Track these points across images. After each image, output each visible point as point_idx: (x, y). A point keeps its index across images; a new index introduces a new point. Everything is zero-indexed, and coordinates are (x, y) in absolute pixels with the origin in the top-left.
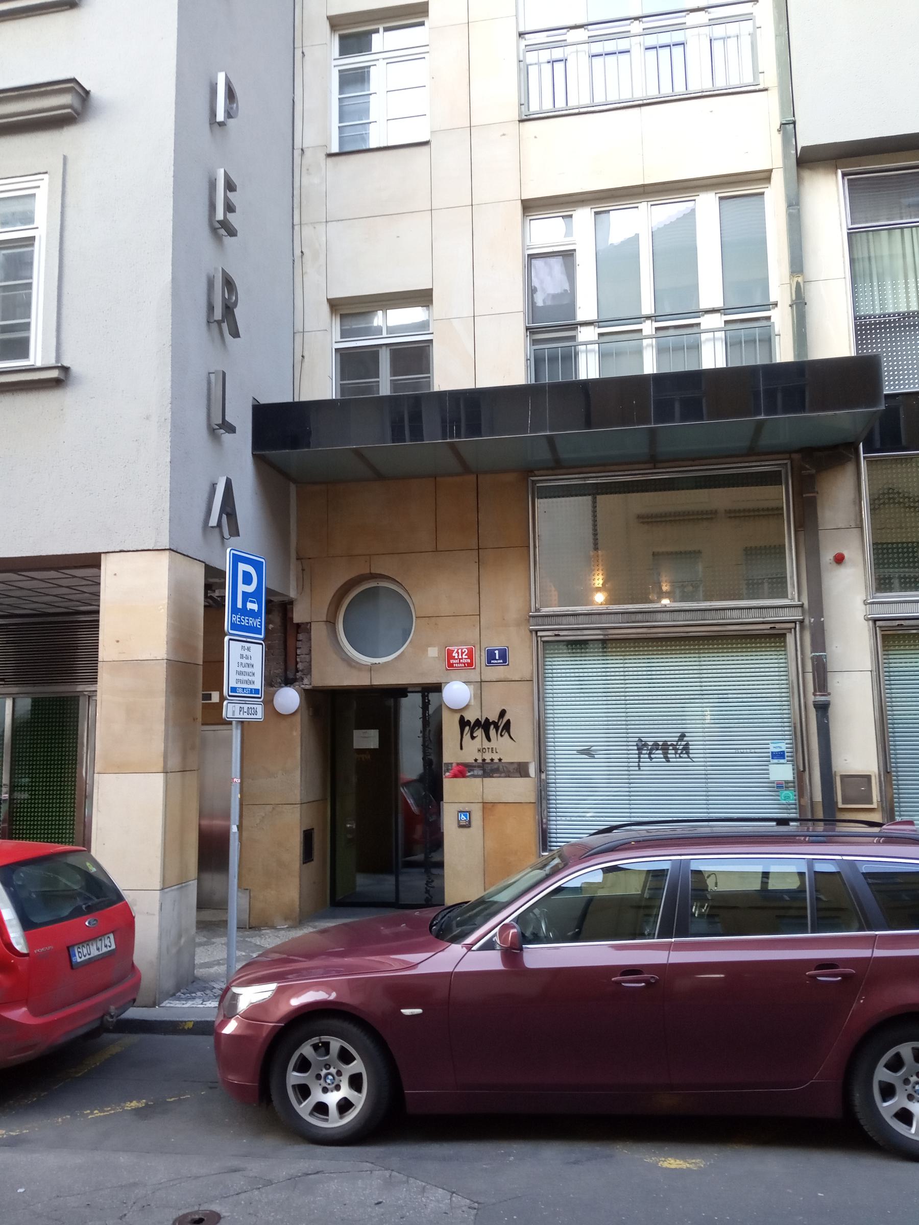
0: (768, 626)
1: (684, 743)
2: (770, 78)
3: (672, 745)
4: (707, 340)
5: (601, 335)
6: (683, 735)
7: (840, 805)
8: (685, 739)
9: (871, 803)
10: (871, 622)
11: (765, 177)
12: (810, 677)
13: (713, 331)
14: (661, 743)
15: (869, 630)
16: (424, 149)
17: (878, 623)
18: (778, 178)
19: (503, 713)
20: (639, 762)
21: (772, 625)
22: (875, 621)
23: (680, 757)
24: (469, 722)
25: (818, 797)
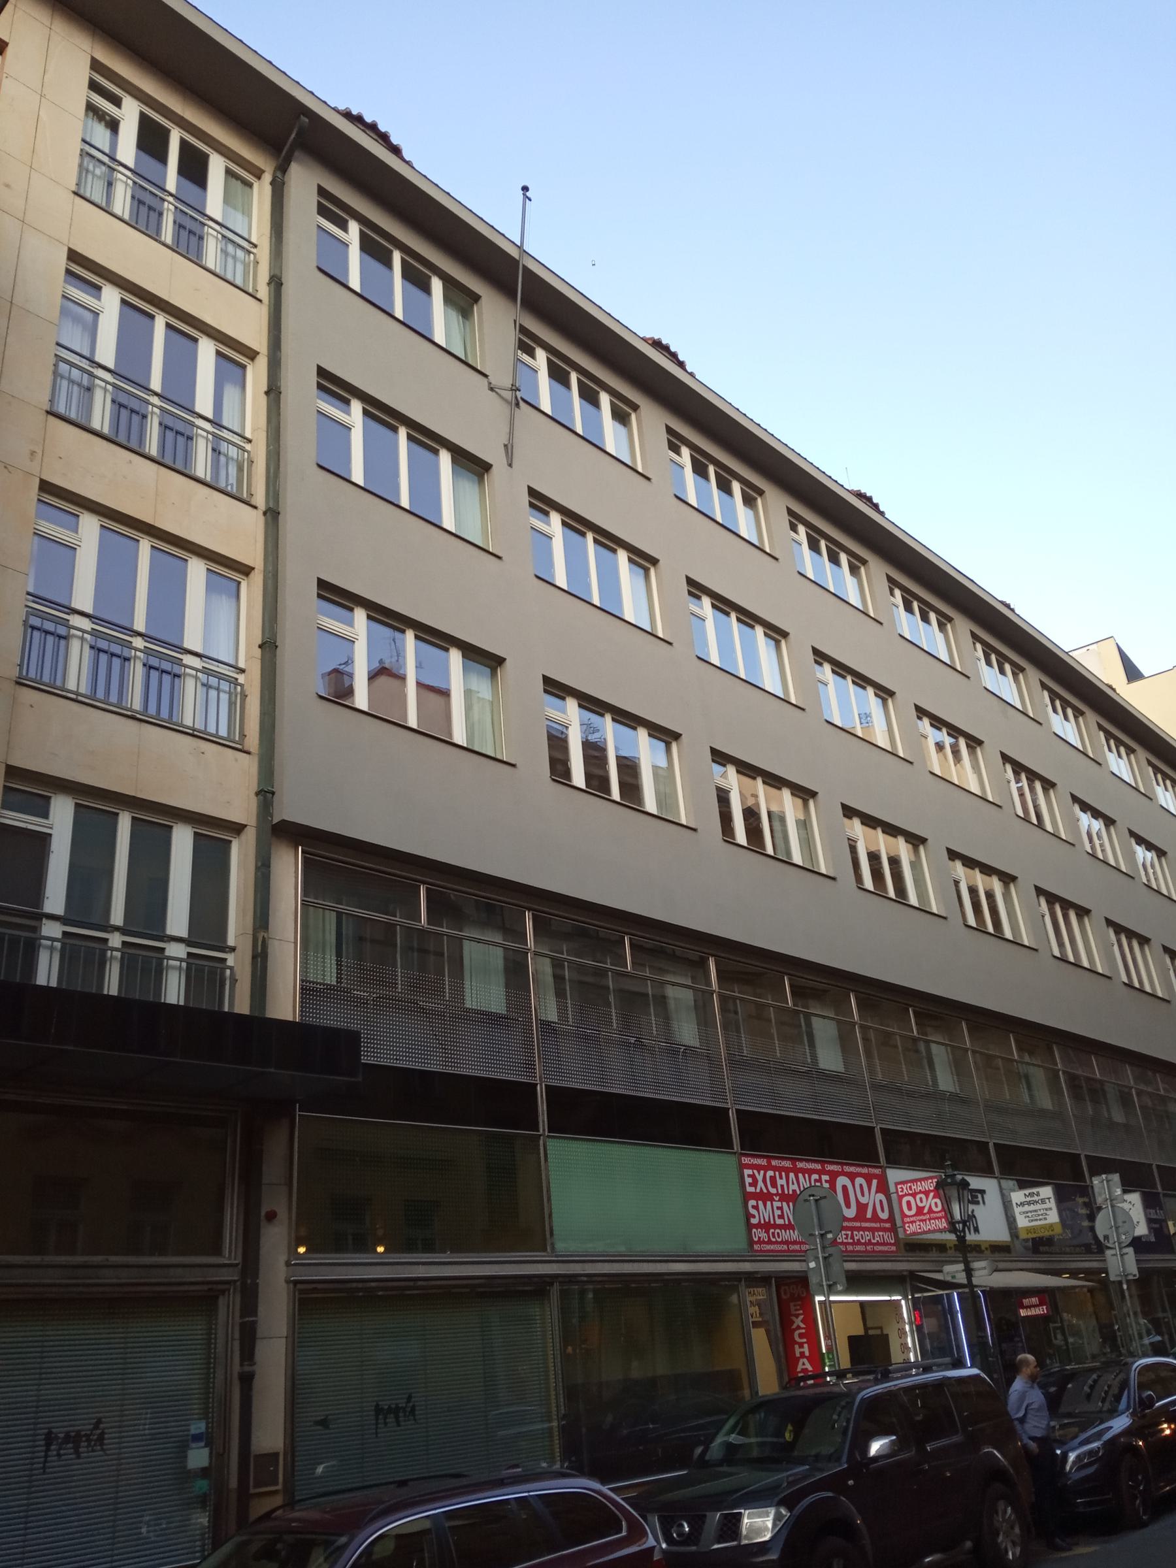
0: (206, 1287)
1: (99, 1432)
2: (253, 740)
3: (86, 1435)
4: (46, 947)
5: (65, 933)
6: (99, 1422)
7: (252, 1491)
8: (102, 1426)
9: (277, 1484)
10: (291, 1285)
11: (238, 829)
12: (237, 1344)
13: (53, 940)
14: (61, 1435)
15: (288, 1294)
16: (1164, 1004)
17: (299, 1286)
18: (250, 835)
19: (409, 1398)
20: (45, 1462)
21: (210, 1286)
22: (296, 1283)
23: (93, 1451)
24: (382, 1409)
25: (233, 1483)
